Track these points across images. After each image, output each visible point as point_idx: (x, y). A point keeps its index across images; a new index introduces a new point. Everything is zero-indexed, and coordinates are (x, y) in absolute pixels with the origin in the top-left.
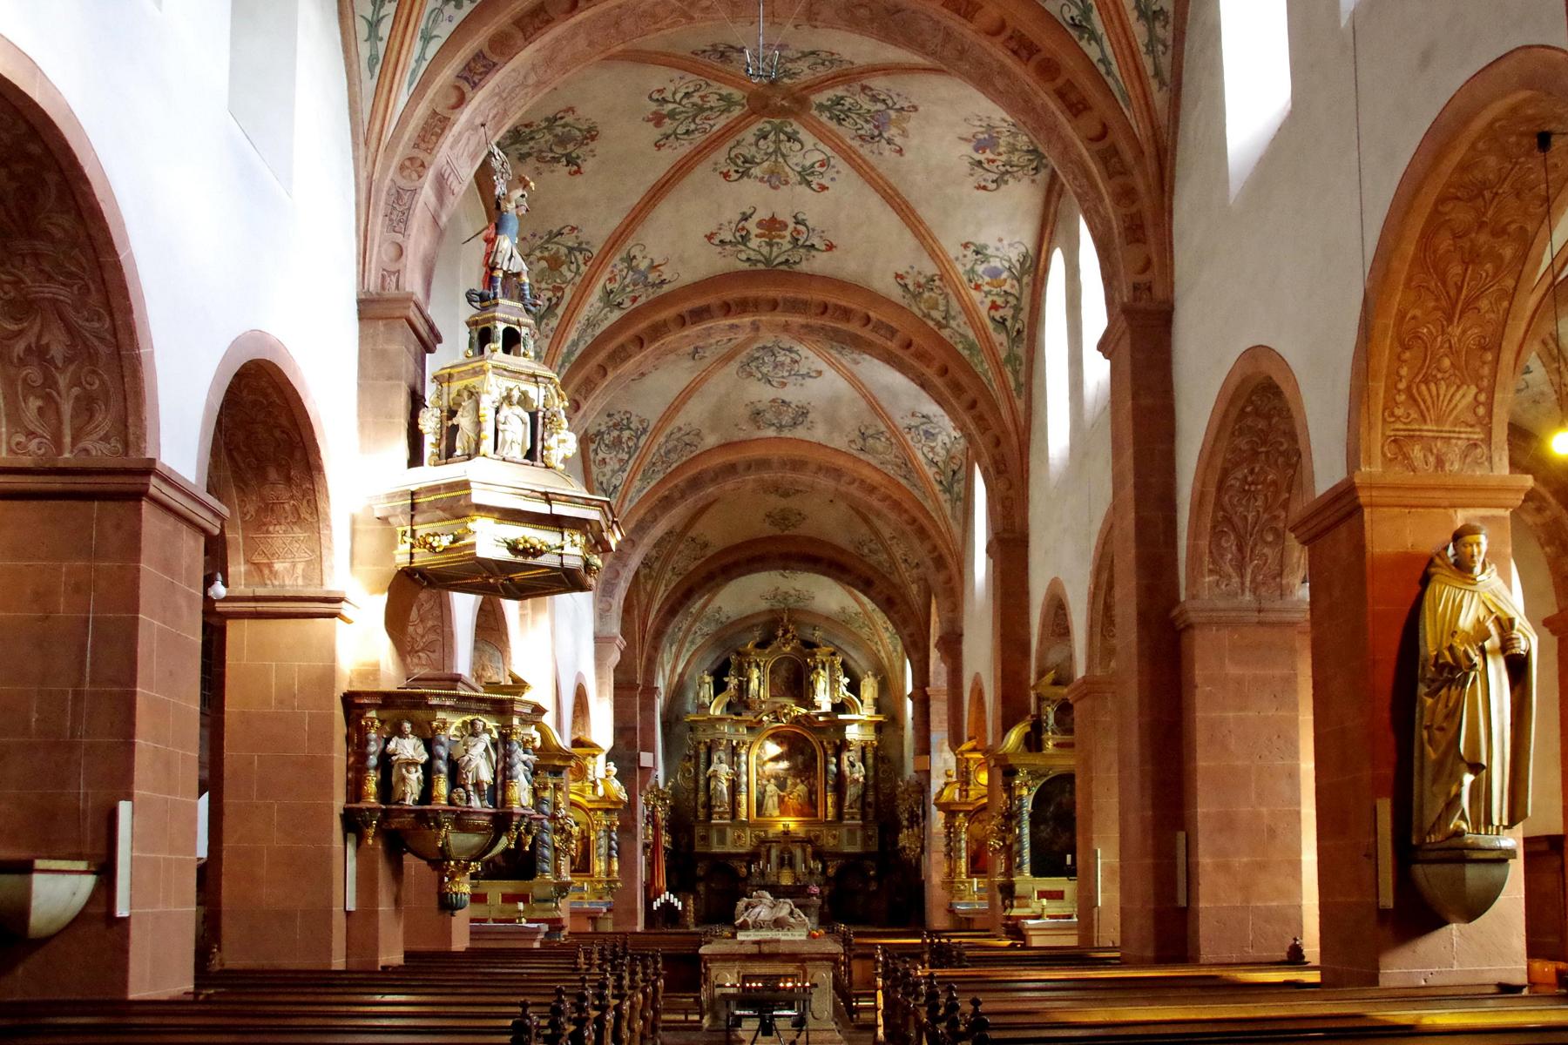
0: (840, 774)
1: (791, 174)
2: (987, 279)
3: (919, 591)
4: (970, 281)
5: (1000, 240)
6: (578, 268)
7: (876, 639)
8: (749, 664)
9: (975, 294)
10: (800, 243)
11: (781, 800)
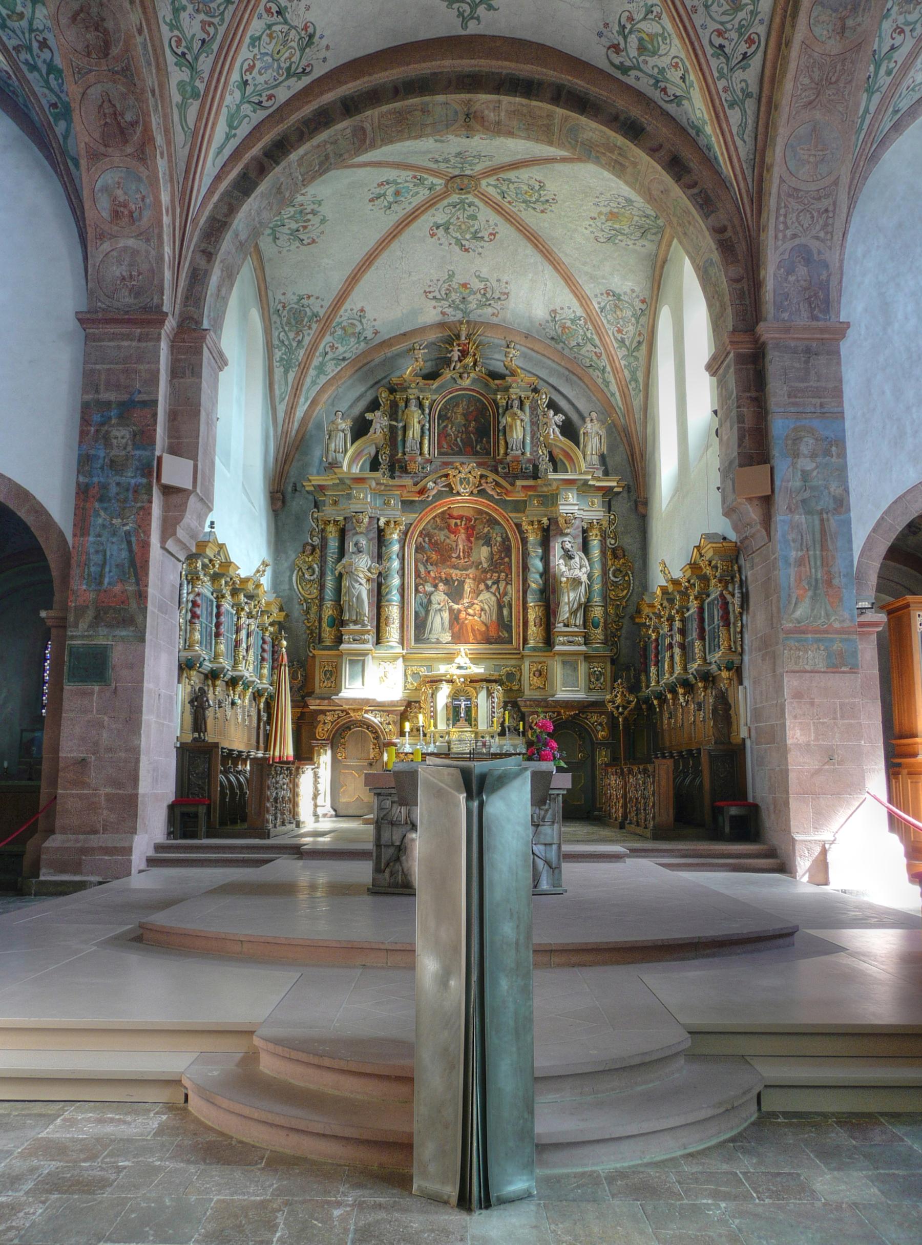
0: (547, 573)
3: (743, 126)
7: (604, 361)
8: (407, 401)
11: (455, 617)
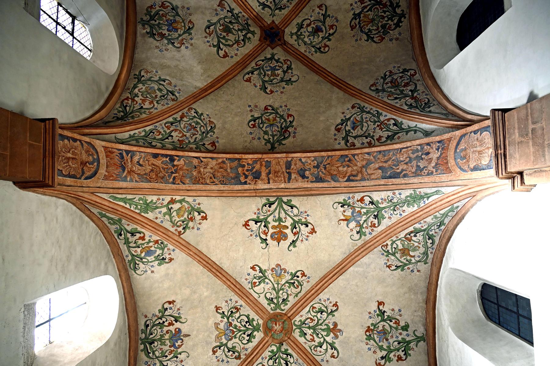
1: (270, 277)
2: (153, 249)
4: (162, 243)
5: (152, 272)
6: (392, 244)
9: (157, 238)
10: (263, 224)
